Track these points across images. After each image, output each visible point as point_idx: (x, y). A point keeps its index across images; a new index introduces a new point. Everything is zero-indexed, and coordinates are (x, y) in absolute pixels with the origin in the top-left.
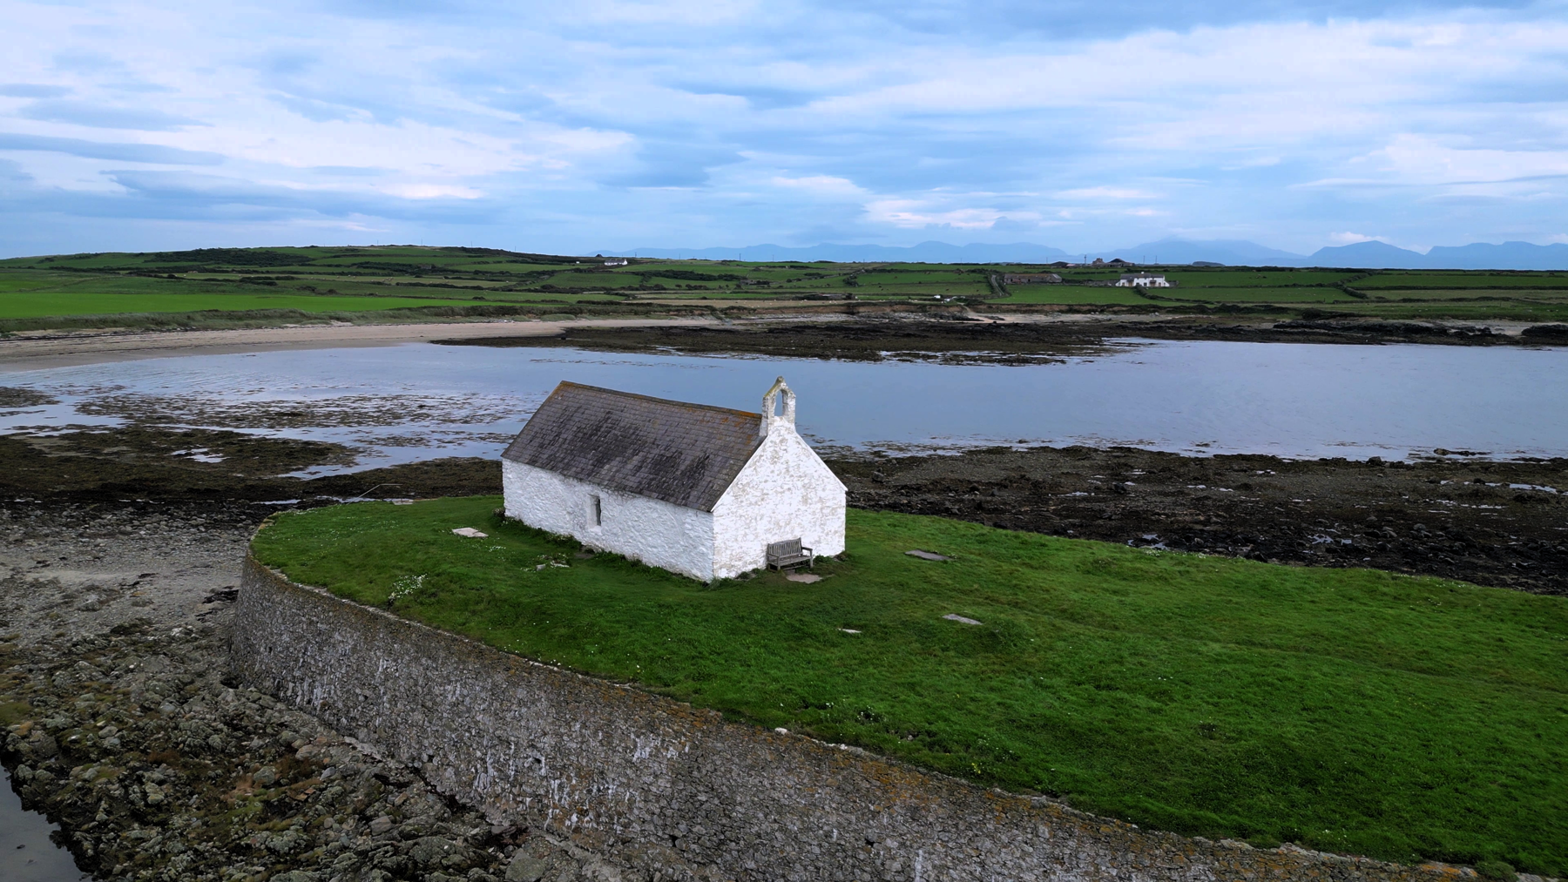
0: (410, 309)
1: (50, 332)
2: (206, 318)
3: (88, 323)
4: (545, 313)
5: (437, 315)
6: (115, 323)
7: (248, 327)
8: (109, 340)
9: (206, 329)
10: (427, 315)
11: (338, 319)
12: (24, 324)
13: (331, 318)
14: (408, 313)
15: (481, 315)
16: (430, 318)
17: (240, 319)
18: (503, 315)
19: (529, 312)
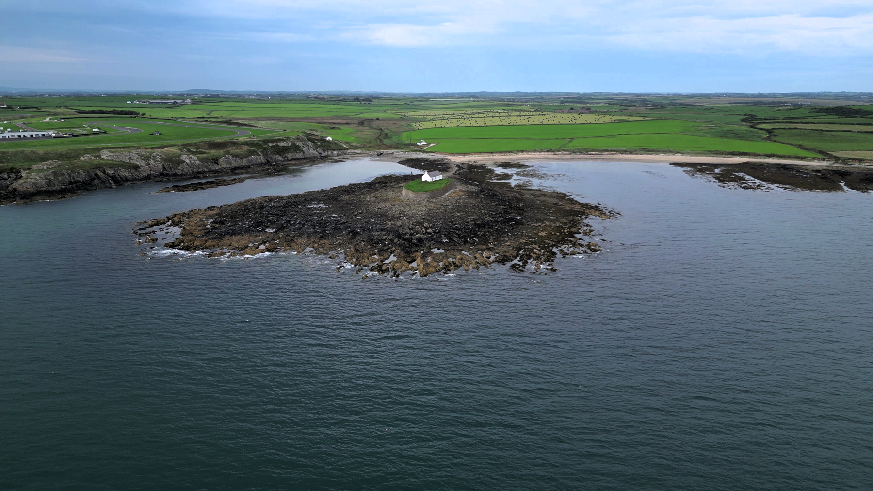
0: (709, 151)
1: (597, 153)
2: (641, 150)
3: (607, 151)
4: (759, 155)
5: (716, 154)
6: (615, 151)
7: (647, 154)
8: (606, 155)
9: (636, 154)
10: (713, 153)
11: (681, 153)
12: (593, 150)
13: (678, 152)
14: (706, 152)
15: (733, 155)
16: (712, 155)
17: (650, 151)
18: (742, 155)
19: (752, 155)
